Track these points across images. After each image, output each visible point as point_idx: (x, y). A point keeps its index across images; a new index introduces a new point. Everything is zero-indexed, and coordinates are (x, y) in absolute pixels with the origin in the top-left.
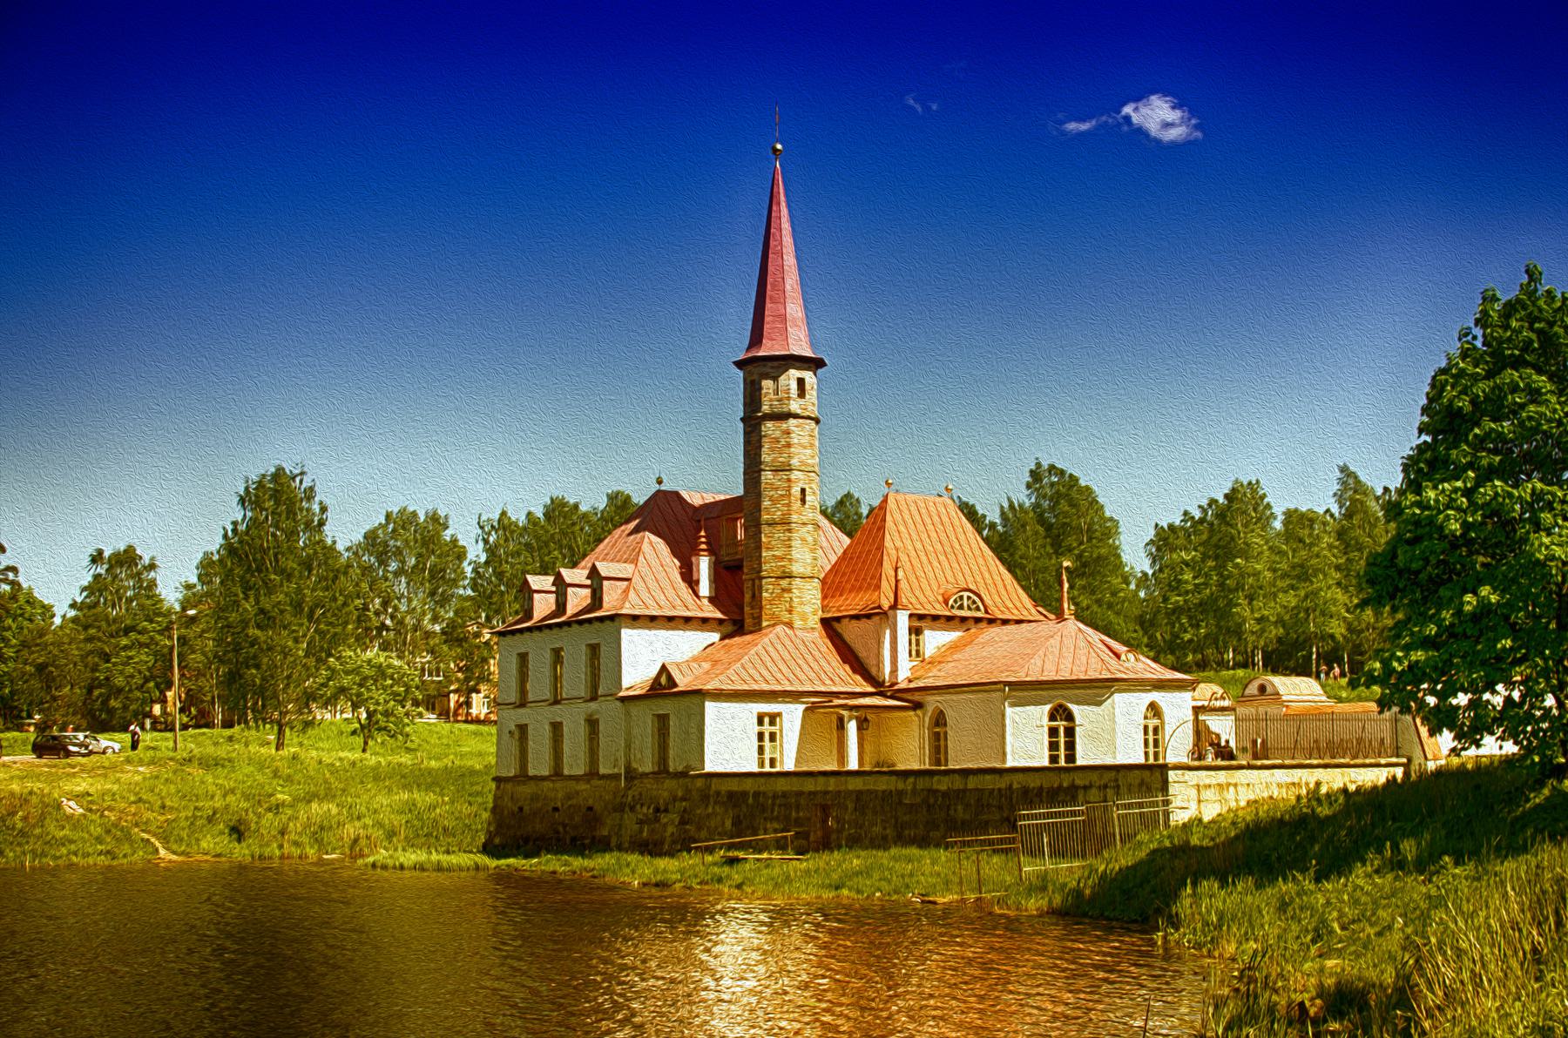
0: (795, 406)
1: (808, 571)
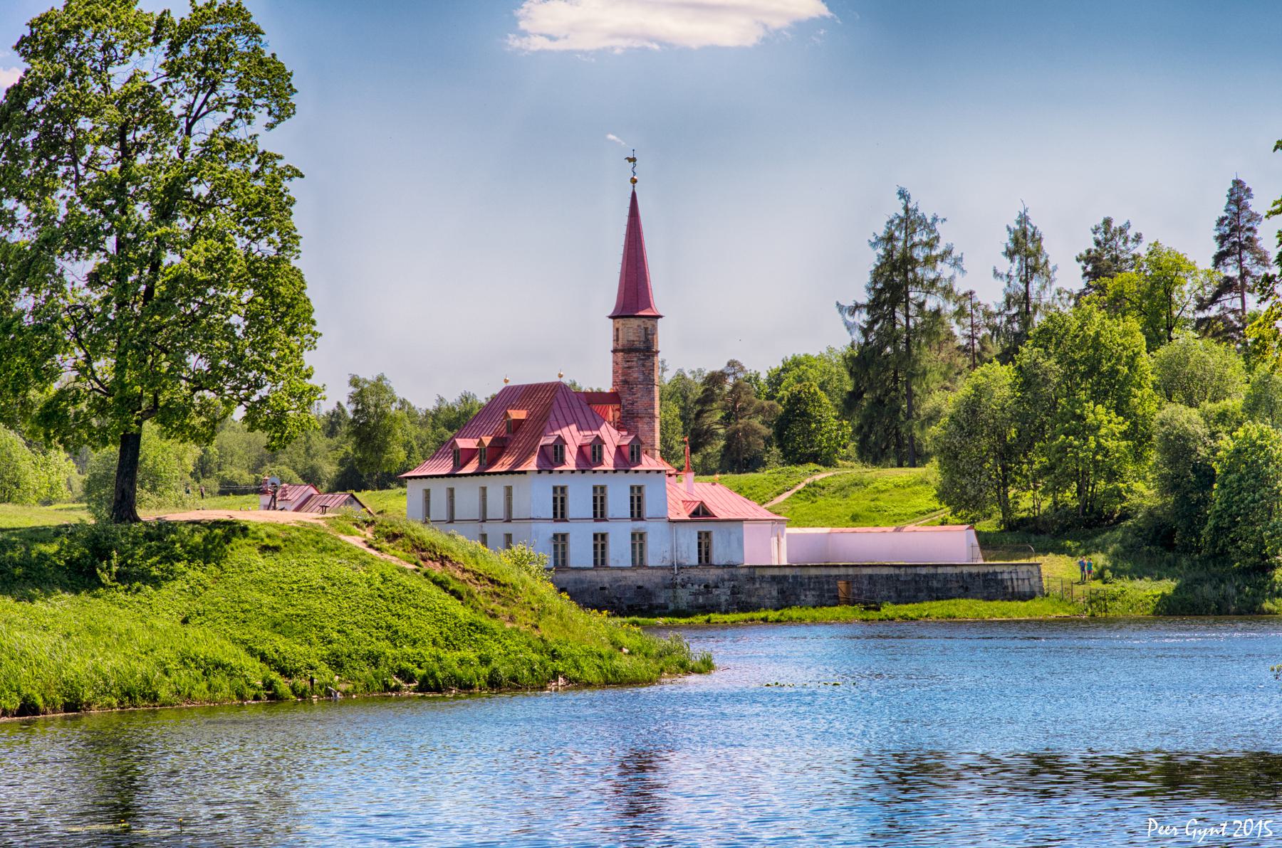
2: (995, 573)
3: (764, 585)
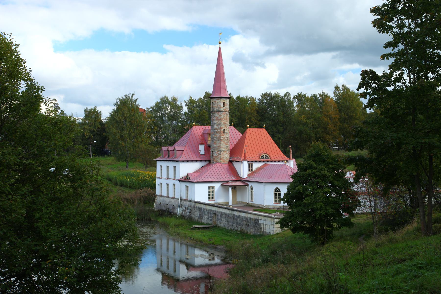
0: (222, 109)
1: (225, 149)
2: (258, 220)
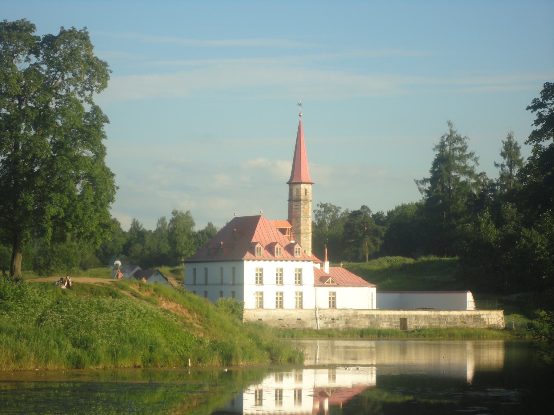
3: (362, 319)
